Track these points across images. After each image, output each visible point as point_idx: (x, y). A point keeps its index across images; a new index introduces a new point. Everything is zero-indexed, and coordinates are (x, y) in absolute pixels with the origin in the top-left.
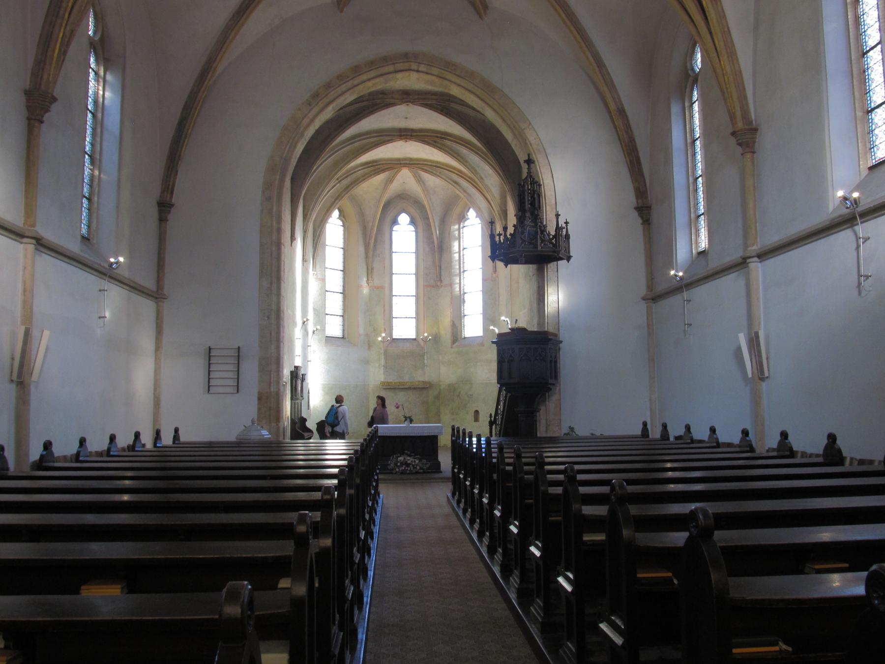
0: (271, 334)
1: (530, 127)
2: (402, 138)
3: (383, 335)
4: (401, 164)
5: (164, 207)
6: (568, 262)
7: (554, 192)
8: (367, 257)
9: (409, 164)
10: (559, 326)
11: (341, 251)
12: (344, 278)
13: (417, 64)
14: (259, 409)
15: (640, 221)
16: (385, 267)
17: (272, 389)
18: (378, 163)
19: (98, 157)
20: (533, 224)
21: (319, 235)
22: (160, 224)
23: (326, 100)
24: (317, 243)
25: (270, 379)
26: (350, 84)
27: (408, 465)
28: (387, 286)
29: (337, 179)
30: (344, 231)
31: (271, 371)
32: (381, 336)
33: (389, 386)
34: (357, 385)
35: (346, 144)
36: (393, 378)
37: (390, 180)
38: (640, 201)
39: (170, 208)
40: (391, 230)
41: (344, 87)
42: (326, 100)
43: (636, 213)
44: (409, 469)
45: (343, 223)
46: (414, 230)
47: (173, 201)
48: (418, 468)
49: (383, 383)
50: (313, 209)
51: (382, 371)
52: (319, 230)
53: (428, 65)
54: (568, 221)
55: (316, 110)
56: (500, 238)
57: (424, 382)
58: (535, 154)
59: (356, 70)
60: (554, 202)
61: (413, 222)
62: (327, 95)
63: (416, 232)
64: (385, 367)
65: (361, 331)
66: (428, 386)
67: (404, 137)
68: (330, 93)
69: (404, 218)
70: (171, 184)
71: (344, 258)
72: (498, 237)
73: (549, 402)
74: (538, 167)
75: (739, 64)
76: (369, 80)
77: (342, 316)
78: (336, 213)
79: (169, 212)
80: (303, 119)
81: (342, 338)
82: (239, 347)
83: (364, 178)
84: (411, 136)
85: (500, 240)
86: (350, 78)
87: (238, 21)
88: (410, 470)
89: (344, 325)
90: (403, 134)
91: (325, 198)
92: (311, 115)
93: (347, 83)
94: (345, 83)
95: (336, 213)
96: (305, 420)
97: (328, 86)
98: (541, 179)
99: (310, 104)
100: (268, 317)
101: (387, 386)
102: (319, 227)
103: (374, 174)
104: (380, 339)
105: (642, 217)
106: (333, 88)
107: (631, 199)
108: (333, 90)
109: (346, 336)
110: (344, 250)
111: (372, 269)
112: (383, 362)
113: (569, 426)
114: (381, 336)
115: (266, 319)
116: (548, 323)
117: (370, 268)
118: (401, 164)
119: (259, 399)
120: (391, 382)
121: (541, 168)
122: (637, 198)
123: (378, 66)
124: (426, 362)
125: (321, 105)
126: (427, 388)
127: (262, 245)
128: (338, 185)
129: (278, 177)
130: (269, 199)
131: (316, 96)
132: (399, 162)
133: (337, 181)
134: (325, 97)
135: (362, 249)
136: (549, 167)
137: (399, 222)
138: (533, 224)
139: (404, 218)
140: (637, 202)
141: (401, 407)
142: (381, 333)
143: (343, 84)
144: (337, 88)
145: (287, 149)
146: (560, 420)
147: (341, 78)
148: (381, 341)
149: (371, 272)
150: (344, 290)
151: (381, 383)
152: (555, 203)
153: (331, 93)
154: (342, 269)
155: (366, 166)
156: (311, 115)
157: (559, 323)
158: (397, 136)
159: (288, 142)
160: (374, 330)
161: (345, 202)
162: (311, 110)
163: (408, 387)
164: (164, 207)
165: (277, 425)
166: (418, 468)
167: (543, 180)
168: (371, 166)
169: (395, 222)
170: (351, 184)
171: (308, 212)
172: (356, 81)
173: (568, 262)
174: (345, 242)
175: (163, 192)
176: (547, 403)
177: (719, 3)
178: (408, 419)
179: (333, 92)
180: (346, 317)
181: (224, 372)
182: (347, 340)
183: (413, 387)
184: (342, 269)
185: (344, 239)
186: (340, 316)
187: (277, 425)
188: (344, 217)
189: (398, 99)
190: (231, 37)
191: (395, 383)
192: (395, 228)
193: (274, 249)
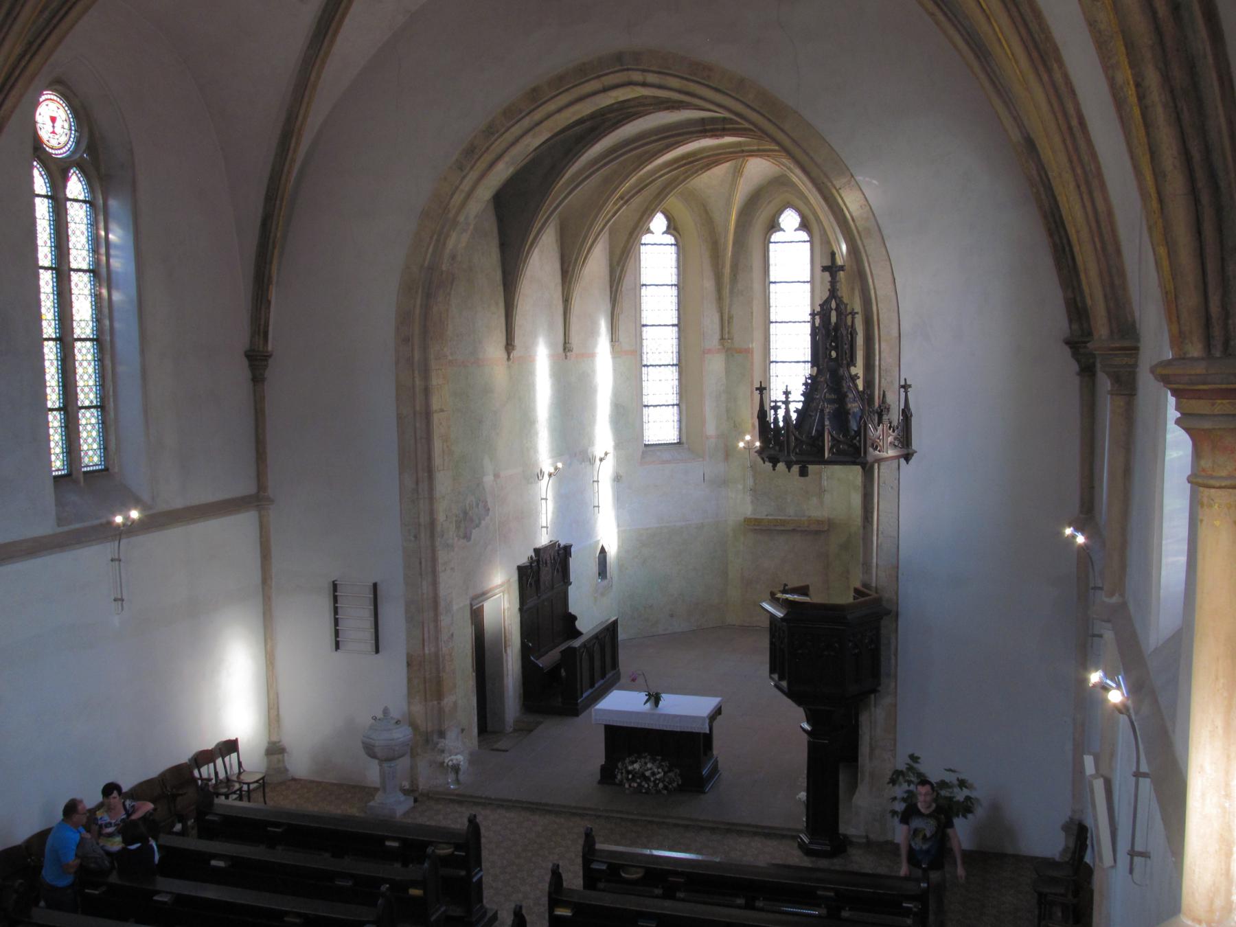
0: (421, 563)
1: (853, 182)
2: (707, 134)
3: (748, 438)
4: (743, 151)
5: (257, 360)
6: (907, 463)
7: (897, 315)
8: (720, 298)
9: (759, 150)
10: (897, 572)
11: (674, 291)
12: (679, 339)
13: (638, 73)
14: (410, 680)
15: (1075, 367)
16: (752, 313)
17: (427, 651)
18: (699, 157)
19: (108, 338)
20: (833, 396)
21: (620, 278)
22: (254, 385)
23: (488, 158)
24: (617, 291)
25: (423, 634)
26: (526, 123)
27: (647, 779)
28: (756, 346)
29: (621, 198)
30: (678, 254)
31: (423, 623)
32: (743, 440)
33: (758, 525)
34: (702, 523)
35: (595, 167)
36: (765, 512)
37: (738, 172)
38: (1075, 326)
39: (266, 360)
40: (766, 243)
41: (516, 130)
42: (488, 158)
43: (1067, 351)
44: (646, 786)
45: (676, 239)
46: (809, 239)
47: (270, 348)
48: (661, 785)
49: (747, 521)
50: (576, 260)
51: (748, 499)
52: (619, 268)
53: (659, 73)
54: (908, 383)
55: (473, 175)
56: (776, 414)
57: (819, 522)
58: (861, 239)
59: (535, 97)
60: (895, 333)
61: (804, 226)
62: (488, 149)
63: (811, 242)
64: (753, 490)
65: (711, 429)
66: (826, 528)
67: (711, 134)
68: (491, 145)
69: (790, 219)
70: (262, 323)
71: (679, 303)
72: (772, 412)
73: (875, 707)
74: (866, 265)
75: (1106, 199)
76: (559, 110)
77: (677, 405)
78: (659, 222)
79: (266, 366)
80: (453, 194)
81: (678, 443)
82: (375, 585)
83: (686, 175)
84: (724, 129)
85: (776, 419)
86: (523, 114)
87: (319, 50)
88: (648, 787)
89: (680, 421)
90: (708, 127)
91: (613, 220)
92: (466, 185)
93: (519, 124)
94: (516, 123)
95: (659, 222)
96: (574, 618)
97: (490, 131)
98: (872, 287)
99: (461, 169)
100: (415, 537)
101: (754, 525)
102: (618, 264)
103: (701, 169)
104: (741, 445)
105: (1078, 361)
106: (496, 135)
107: (1058, 321)
108: (498, 138)
109: (684, 440)
110: (678, 289)
111: (730, 318)
112: (750, 482)
113: (910, 753)
114: (743, 440)
115: (413, 539)
116: (877, 564)
117: (726, 317)
118: (743, 151)
119: (409, 665)
120: (763, 519)
121: (872, 266)
122: (1070, 321)
123: (571, 85)
124: (825, 483)
125: (481, 165)
126: (825, 531)
127: (400, 417)
128: (624, 208)
129: (419, 302)
130: (407, 340)
131: (471, 152)
132: (739, 149)
133: (622, 202)
134: (485, 152)
135: (709, 284)
136: (888, 263)
137: (782, 226)
138: (833, 396)
139: (790, 219)
140: (1070, 328)
141: (640, 680)
142: (744, 434)
143: (513, 125)
144: (504, 133)
145: (430, 250)
146: (895, 740)
147: (511, 114)
148: (744, 447)
149: (729, 323)
150: (679, 359)
151: (745, 521)
152: (897, 335)
153: (494, 146)
154: (675, 322)
155: (675, 166)
156: (466, 185)
157: (898, 567)
158: (701, 132)
159: (431, 238)
160: (735, 426)
161: (672, 201)
162: (464, 177)
163: (790, 529)
164: (257, 360)
165: (439, 703)
166: (661, 785)
167: (875, 288)
168: (685, 165)
169: (774, 226)
170: (664, 188)
171: (569, 266)
172: (537, 116)
173: (907, 463)
174: (679, 275)
175: (253, 336)
176: (873, 709)
177: (1055, 66)
178: (653, 698)
179: (497, 143)
180: (684, 407)
181: (357, 621)
182: (686, 446)
183: (799, 529)
184: (675, 322)
185: (678, 267)
186: (673, 405)
187: (439, 703)
188: (675, 229)
189: (651, 105)
190: (312, 79)
191: (769, 521)
192: (776, 237)
193: (418, 425)
